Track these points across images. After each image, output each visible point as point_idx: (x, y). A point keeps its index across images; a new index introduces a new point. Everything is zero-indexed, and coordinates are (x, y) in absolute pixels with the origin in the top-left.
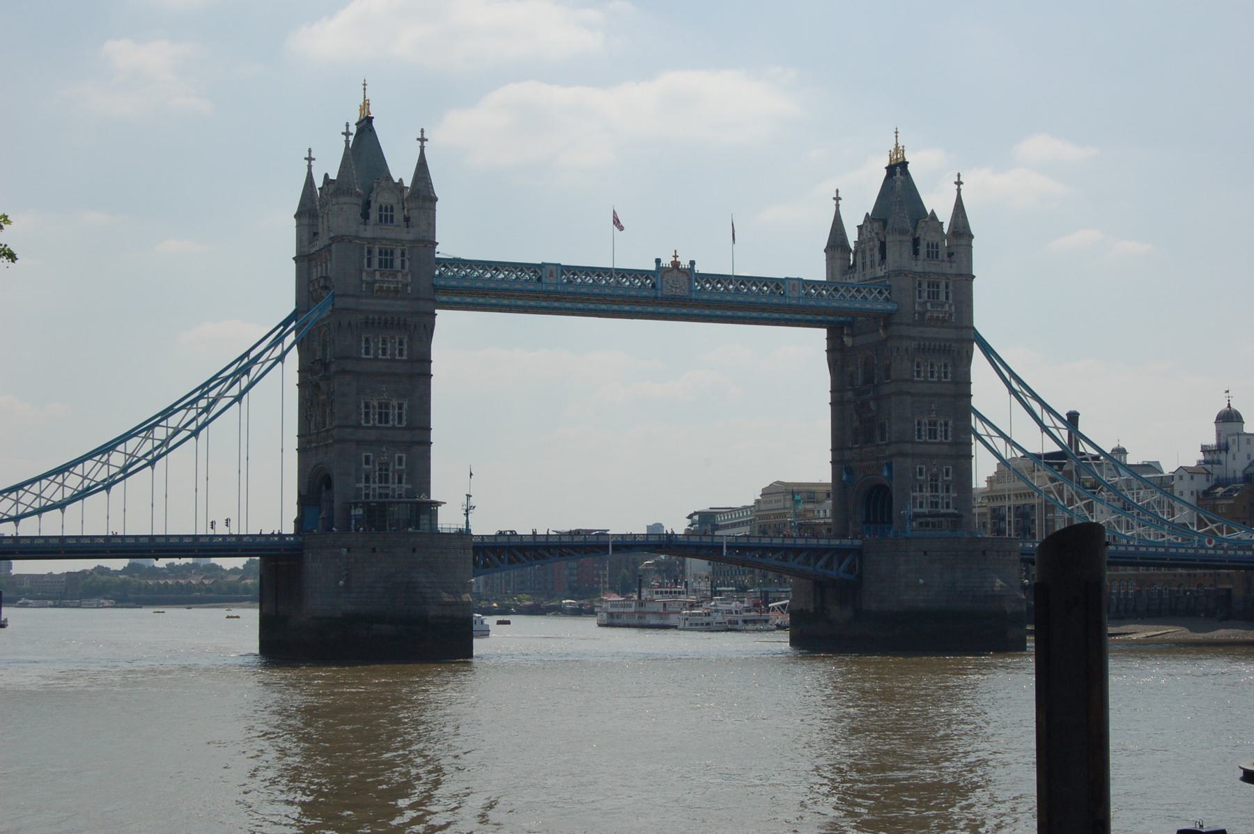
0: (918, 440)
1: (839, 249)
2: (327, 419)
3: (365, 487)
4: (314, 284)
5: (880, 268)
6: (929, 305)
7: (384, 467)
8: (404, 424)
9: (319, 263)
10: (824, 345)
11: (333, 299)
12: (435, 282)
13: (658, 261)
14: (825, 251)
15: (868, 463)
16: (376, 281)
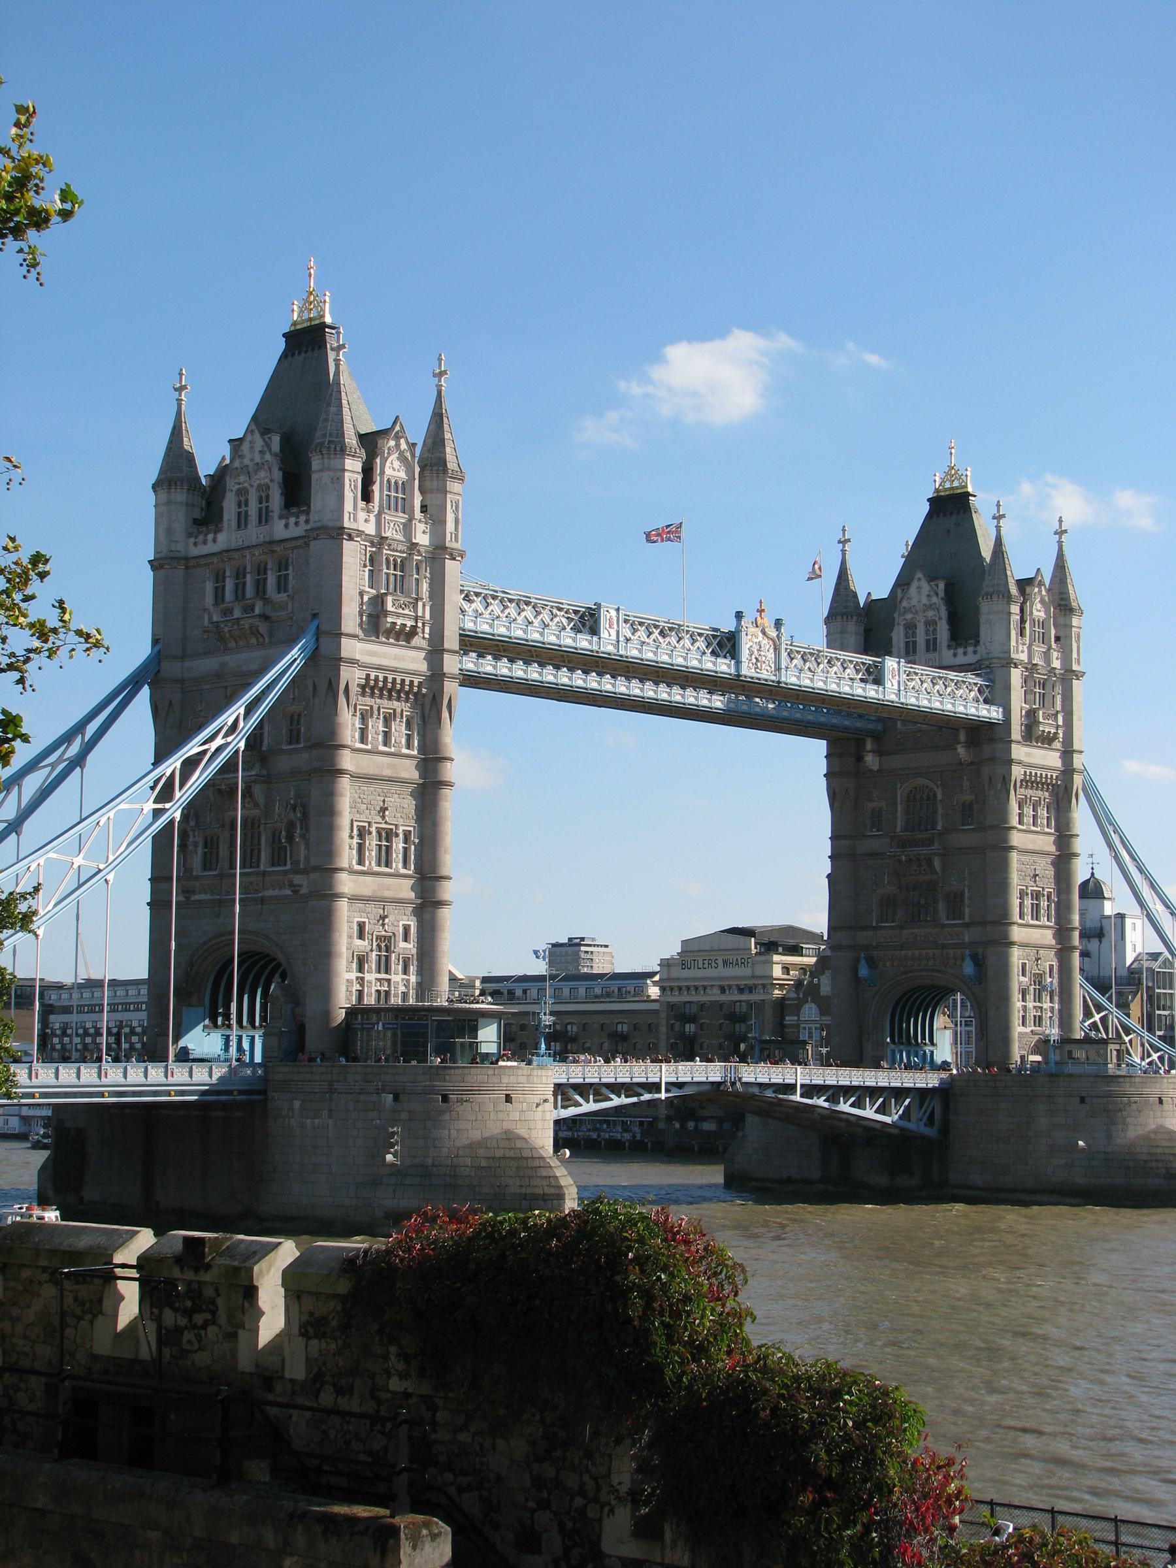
0: (1020, 921)
1: (855, 618)
2: (263, 855)
3: (357, 978)
4: (228, 612)
5: (952, 651)
6: (1041, 712)
7: (386, 944)
8: (412, 868)
9: (228, 574)
10: (822, 766)
11: (317, 640)
12: (462, 625)
13: (739, 615)
14: (828, 620)
15: (917, 952)
16: (386, 613)
